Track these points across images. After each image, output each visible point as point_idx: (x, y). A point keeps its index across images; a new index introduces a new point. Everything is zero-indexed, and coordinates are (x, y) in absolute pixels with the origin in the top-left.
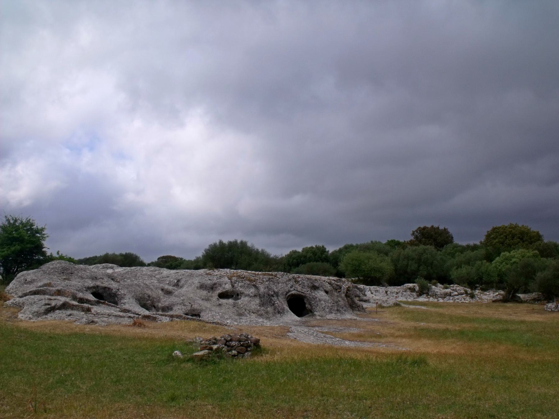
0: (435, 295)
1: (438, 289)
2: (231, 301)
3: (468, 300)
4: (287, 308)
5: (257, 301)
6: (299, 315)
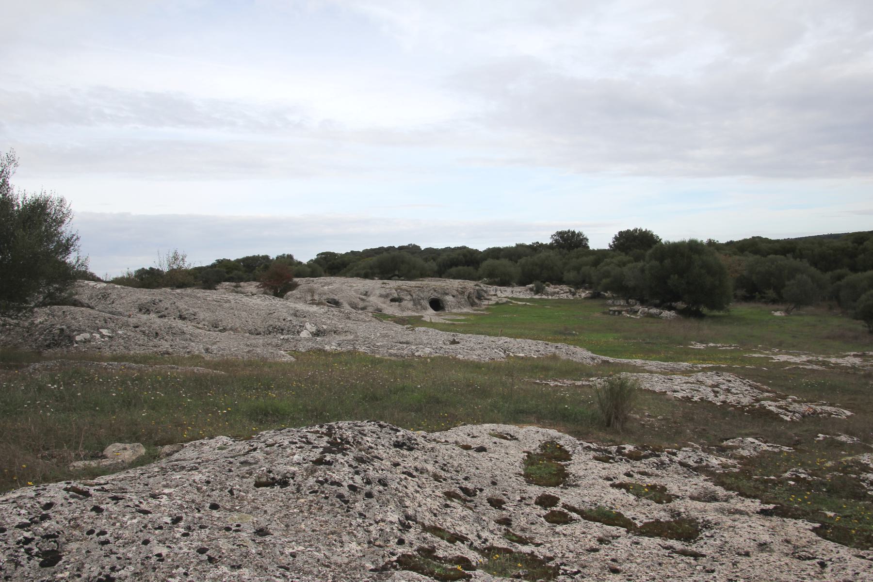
0: (547, 294)
1: (550, 289)
2: (397, 303)
3: (571, 297)
4: (429, 306)
5: (412, 303)
6: (435, 310)
